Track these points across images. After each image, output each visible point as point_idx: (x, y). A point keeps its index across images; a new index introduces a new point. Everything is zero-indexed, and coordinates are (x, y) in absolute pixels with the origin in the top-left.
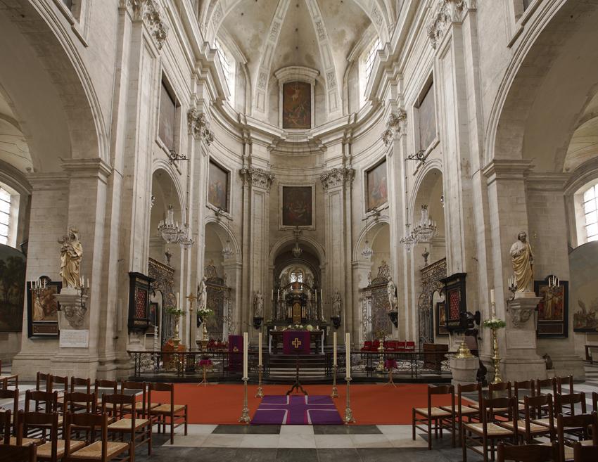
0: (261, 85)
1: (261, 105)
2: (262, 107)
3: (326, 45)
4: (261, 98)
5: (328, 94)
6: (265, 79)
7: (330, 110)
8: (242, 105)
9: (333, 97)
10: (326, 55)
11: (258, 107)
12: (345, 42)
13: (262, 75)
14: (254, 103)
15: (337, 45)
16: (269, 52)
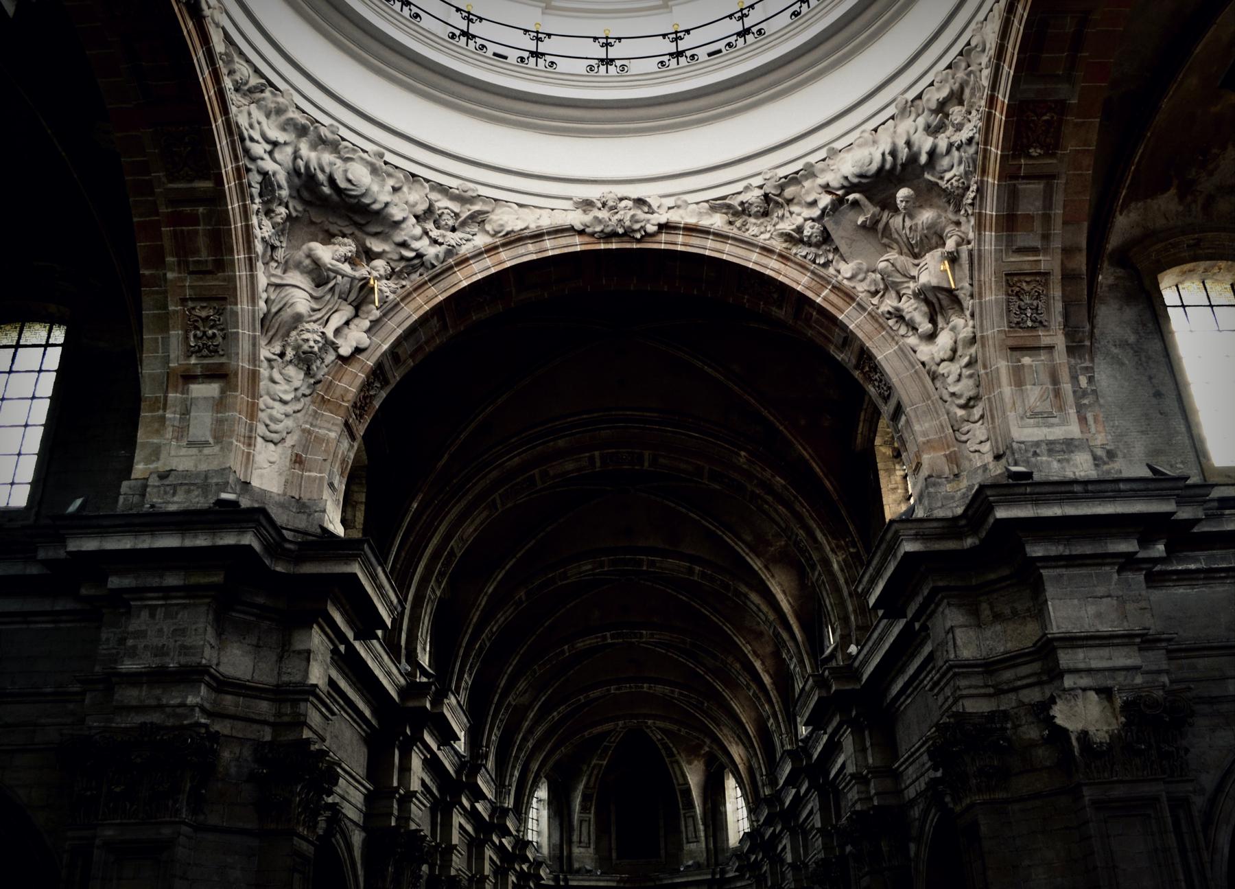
0: (584, 809)
1: (584, 838)
2: (586, 840)
3: (678, 762)
4: (585, 826)
5: (683, 819)
6: (591, 801)
7: (687, 838)
8: (558, 843)
9: (690, 822)
10: (678, 773)
11: (580, 842)
12: (703, 752)
13: (586, 798)
14: (575, 838)
15: (693, 757)
16: (595, 772)
